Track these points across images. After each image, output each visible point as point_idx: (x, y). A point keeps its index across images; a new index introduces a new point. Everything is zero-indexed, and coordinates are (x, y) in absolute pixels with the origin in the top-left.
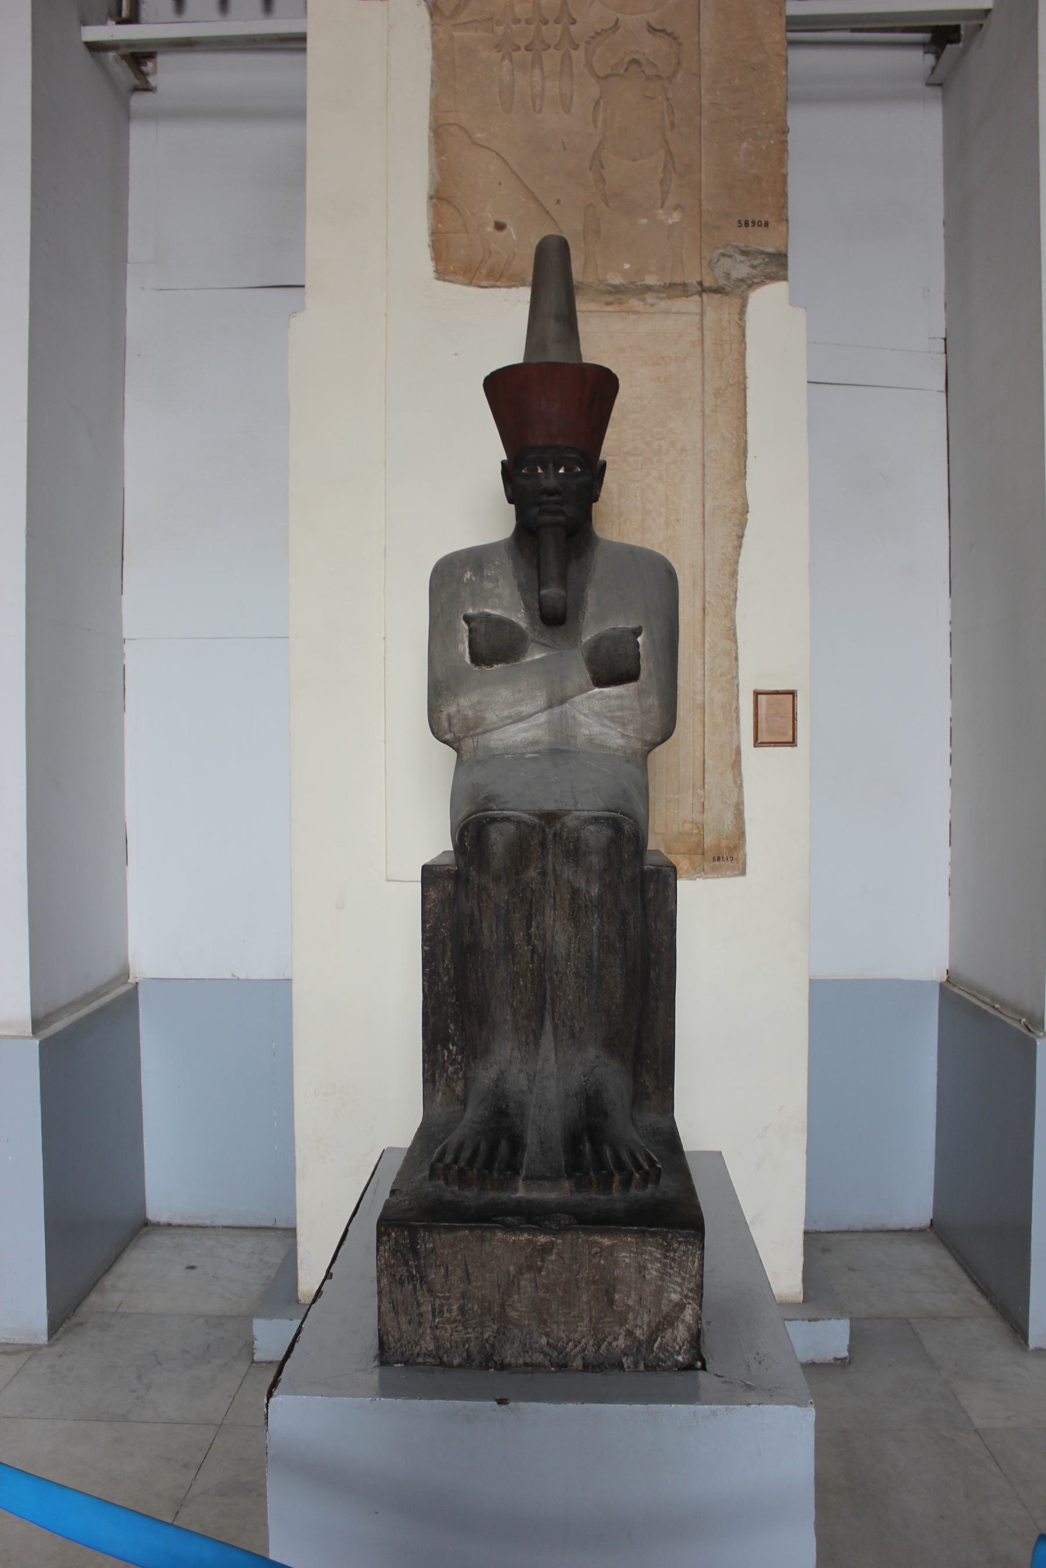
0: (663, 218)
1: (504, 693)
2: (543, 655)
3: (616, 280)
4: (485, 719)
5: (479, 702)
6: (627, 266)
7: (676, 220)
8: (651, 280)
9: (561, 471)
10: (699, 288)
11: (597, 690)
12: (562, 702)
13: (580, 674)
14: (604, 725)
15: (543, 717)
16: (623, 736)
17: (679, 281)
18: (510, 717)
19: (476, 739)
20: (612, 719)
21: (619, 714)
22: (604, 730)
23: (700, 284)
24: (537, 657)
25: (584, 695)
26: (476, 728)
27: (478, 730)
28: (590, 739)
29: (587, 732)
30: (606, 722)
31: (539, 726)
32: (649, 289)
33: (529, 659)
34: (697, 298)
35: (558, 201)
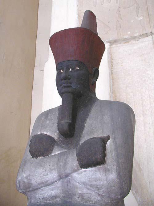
0: (138, 19)
1: (40, 171)
2: (60, 152)
3: (127, 37)
4: (32, 184)
5: (29, 175)
6: (129, 33)
7: (141, 19)
8: (136, 35)
9: (71, 70)
10: (151, 34)
11: (83, 170)
12: (67, 176)
13: (73, 160)
14: (88, 189)
15: (59, 184)
16: (99, 195)
17: (144, 32)
18: (42, 183)
19: (31, 193)
20: (91, 186)
21: (94, 183)
22: (89, 191)
23: (151, 32)
24: (57, 153)
25: (77, 173)
26: (29, 188)
27: (30, 189)
28: (82, 196)
29: (80, 192)
30: (89, 187)
31: (58, 188)
32: (136, 37)
33: (53, 154)
34: (151, 36)
35: (109, 22)
